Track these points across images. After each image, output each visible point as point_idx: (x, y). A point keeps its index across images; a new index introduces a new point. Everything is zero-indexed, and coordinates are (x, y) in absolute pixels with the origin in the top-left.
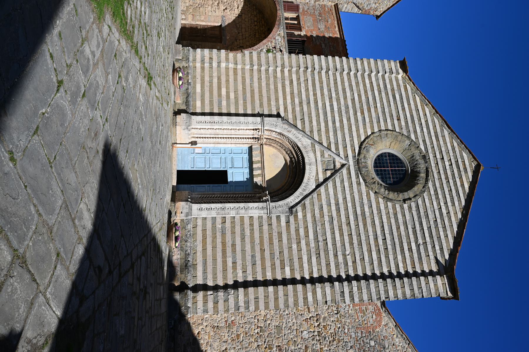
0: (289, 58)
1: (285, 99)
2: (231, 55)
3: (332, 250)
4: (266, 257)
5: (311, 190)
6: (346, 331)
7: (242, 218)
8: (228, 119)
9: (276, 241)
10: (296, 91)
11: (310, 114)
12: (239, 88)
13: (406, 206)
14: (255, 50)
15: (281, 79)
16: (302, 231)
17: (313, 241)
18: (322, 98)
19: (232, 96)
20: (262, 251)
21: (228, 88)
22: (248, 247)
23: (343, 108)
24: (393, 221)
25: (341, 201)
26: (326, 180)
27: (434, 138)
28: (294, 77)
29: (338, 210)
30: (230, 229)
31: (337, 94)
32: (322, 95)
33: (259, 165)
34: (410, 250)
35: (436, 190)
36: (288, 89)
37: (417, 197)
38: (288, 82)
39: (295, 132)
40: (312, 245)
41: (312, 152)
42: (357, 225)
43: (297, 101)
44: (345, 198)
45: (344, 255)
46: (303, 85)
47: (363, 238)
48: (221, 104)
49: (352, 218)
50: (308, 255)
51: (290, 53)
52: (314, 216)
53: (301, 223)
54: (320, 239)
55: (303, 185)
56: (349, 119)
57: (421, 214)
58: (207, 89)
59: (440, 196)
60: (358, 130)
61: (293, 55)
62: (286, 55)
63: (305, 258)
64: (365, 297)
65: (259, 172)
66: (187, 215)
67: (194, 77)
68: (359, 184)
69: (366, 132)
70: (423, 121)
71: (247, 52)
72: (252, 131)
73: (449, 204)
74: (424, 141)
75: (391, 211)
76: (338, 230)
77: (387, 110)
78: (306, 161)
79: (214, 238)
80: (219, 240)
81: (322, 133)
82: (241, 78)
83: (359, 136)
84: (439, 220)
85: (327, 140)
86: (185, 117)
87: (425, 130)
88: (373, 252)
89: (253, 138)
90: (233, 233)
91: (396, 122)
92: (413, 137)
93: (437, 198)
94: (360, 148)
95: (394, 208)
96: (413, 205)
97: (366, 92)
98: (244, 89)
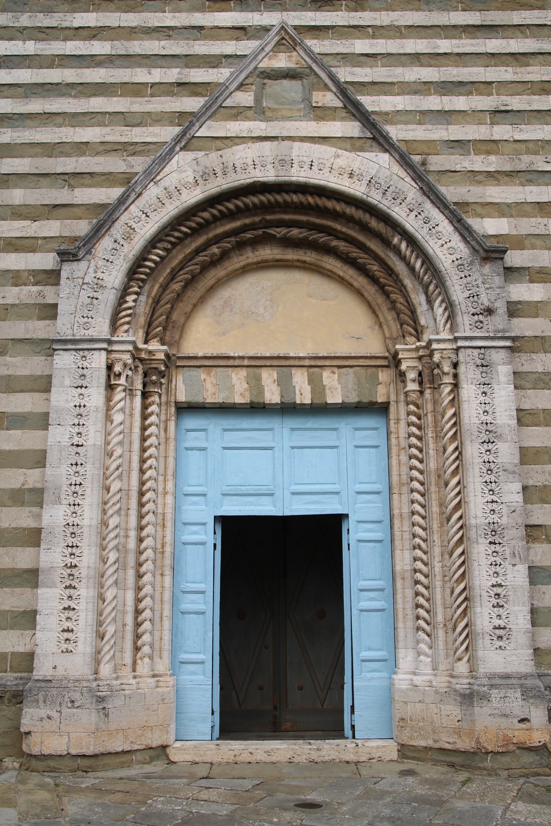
8: (58, 501)
39: (132, 207)
44: (417, 59)
49: (494, 45)
52: (494, 177)
55: (375, 198)
72: (119, 395)
76: (544, 98)
78: (269, 175)
85: (171, 94)
86: (43, 712)
89: (145, 395)
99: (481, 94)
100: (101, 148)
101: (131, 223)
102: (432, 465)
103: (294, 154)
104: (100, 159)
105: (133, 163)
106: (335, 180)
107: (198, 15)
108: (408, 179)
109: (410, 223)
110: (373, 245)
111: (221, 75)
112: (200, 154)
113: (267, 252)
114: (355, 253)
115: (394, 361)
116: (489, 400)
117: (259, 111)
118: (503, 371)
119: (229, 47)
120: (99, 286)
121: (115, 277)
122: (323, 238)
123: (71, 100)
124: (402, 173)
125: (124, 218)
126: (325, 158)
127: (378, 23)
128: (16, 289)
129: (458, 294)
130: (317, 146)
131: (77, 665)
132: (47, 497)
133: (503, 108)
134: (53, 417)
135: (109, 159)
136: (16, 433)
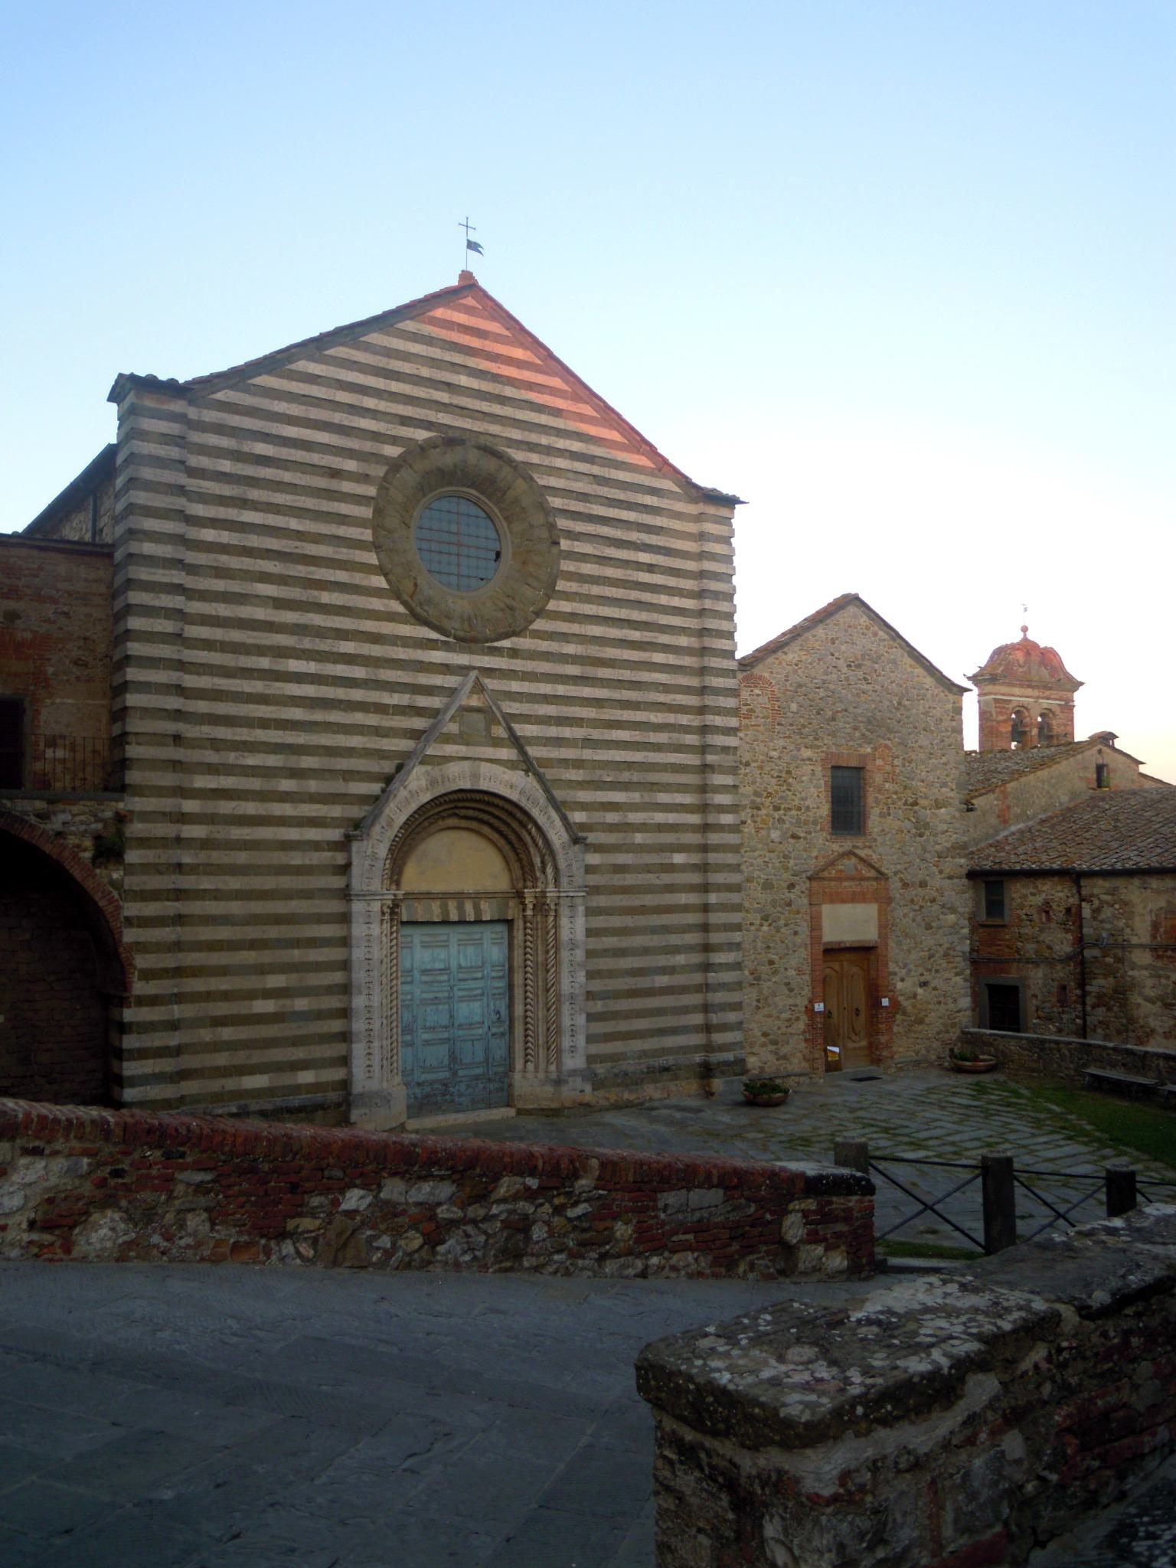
0: (140, 791)
2: (139, 987)
8: (360, 993)
10: (255, 784)
12: (251, 961)
13: (565, 544)
14: (118, 908)
16: (612, 817)
20: (643, 910)
21: (251, 995)
22: (638, 941)
23: (307, 643)
24: (596, 590)
26: (517, 742)
27: (395, 386)
28: (201, 782)
30: (607, 981)
31: (260, 650)
33: (452, 905)
34: (651, 568)
36: (251, 808)
38: (222, 803)
39: (392, 805)
40: (636, 797)
41: (444, 767)
43: (287, 785)
44: (546, 699)
46: (232, 757)
47: (626, 675)
49: (587, 692)
51: (123, 788)
53: (598, 817)
54: (625, 776)
55: (523, 803)
58: (258, 1057)
59: (544, 440)
61: (133, 777)
62: (137, 804)
63: (660, 817)
64: (731, 703)
65: (469, 907)
66: (585, 1079)
67: (219, 1097)
68: (514, 653)
69: (378, 593)
70: (342, 397)
71: (129, 935)
74: (405, 421)
75: (573, 587)
77: (310, 503)
78: (468, 786)
80: (625, 1005)
83: (391, 617)
84: (596, 470)
85: (403, 714)
86: (363, 1111)
87: (370, 403)
88: (655, 660)
92: (392, 451)
93: (549, 450)
95: (571, 576)
96: (562, 523)
98: (253, 945)
102: (540, 959)
107: (419, 651)
109: (541, 820)
110: (515, 825)
111: (435, 702)
112: (429, 768)
113: (451, 822)
114: (503, 828)
115: (520, 895)
116: (573, 927)
117: (461, 739)
118: (581, 909)
119: (438, 680)
120: (374, 857)
121: (383, 851)
122: (486, 817)
123: (342, 713)
124: (538, 787)
125: (387, 811)
126: (504, 780)
128: (317, 854)
129: (562, 864)
131: (373, 1085)
132: (354, 990)
134: (354, 942)
136: (325, 950)
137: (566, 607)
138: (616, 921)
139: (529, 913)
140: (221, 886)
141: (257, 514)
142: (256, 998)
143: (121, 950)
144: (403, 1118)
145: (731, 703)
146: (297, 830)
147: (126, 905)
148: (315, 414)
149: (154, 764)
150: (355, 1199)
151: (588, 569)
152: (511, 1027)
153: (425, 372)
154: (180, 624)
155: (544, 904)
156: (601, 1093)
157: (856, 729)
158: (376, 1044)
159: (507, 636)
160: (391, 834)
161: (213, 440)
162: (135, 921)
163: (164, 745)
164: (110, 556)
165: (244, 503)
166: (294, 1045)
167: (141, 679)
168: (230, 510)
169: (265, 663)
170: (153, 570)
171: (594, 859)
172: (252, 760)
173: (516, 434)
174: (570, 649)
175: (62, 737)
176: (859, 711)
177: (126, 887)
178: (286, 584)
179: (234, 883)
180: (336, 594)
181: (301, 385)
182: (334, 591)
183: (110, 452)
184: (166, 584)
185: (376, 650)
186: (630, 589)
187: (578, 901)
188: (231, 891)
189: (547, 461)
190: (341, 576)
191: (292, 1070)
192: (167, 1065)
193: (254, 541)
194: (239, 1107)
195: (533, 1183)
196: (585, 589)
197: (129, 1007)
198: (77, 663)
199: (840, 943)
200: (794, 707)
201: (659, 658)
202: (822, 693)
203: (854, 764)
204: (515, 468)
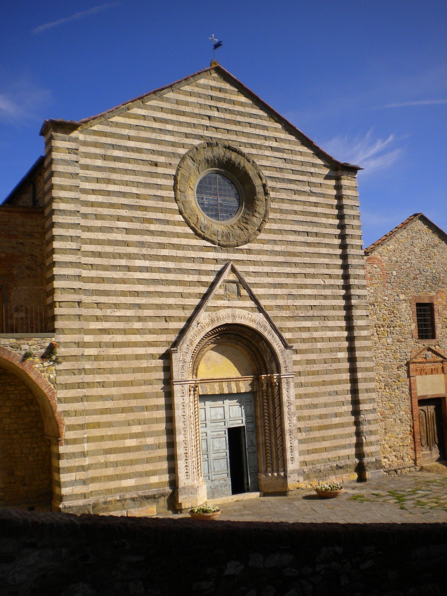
0: (63, 331)
1: (135, 344)
2: (67, 435)
3: (321, 301)
4: (330, 380)
5: (265, 319)
6: (386, 298)
7: (300, 408)
8: (180, 433)
9: (316, 367)
11: (159, 307)
13: (272, 194)
14: (54, 393)
15: (99, 349)
16: (305, 335)
17: (314, 322)
18: (130, 283)
19: (137, 429)
20: (324, 383)
21: (124, 437)
23: (144, 251)
24: (290, 217)
25: (270, 280)
26: (253, 297)
28: (94, 325)
29: (281, 286)
30: (308, 422)
31: (120, 256)
32: (124, 281)
35: (252, 146)
36: (119, 338)
37: (261, 175)
38: (105, 336)
39: (192, 333)
40: (316, 323)
42: (296, 264)
43: (137, 325)
44: (268, 274)
45: (325, 287)
46: (108, 312)
47: (307, 260)
48: (151, 445)
49: (288, 270)
50: (326, 330)
51: (54, 331)
54: (311, 313)
56: (162, 246)
57: (280, 176)
58: (129, 469)
59: (259, 142)
60: (178, 235)
61: (58, 324)
63: (329, 334)
64: (362, 272)
65: (233, 385)
67: (109, 491)
68: (249, 251)
71: (60, 408)
73: (266, 133)
74: (187, 135)
75: (278, 216)
77: (142, 179)
78: (230, 321)
79: (314, 440)
80: (317, 434)
81: (185, 291)
82: (105, 416)
85: (195, 286)
86: (184, 497)
87: (169, 127)
90: (310, 418)
91: (160, 170)
92: (182, 151)
93: (260, 147)
94: (204, 238)
95: (275, 210)
97: (112, 206)
98: (123, 410)
99: (284, 288)
100: (175, 306)
101: (192, 339)
102: (271, 412)
103: (237, 313)
104: (175, 311)
105: (186, 313)
106: (248, 322)
107: (201, 253)
108: (268, 322)
112: (210, 313)
118: (292, 384)
121: (188, 358)
123: (164, 287)
127: (256, 260)
129: (281, 361)
130: (243, 310)
133: (291, 294)
135: (178, 311)
137: (275, 226)
138: (310, 390)
139: (264, 388)
140: (106, 380)
141: (116, 186)
142: (127, 439)
143: (56, 415)
144: (206, 499)
145: (362, 272)
146: (144, 348)
147: (59, 391)
148: (144, 134)
149: (68, 317)
150: (232, 568)
151: (285, 206)
152: (258, 449)
153: (197, 111)
154: (79, 244)
155: (272, 383)
156: (306, 482)
157: (427, 283)
158: (190, 461)
159: (246, 243)
160: (192, 348)
161: (93, 150)
162: (63, 400)
163: (74, 307)
164: (43, 213)
165: (109, 181)
166: (148, 462)
167: (61, 273)
168: (102, 185)
169: (123, 262)
170: (65, 217)
171: (297, 357)
172: (119, 313)
173: (244, 140)
174: (278, 248)
175: (21, 306)
176: (428, 274)
177: (58, 382)
178: (132, 221)
179: (113, 378)
180: (157, 225)
181: (135, 120)
182: (157, 224)
183: (42, 160)
184: (72, 224)
185: (180, 253)
186: (307, 215)
187: (291, 380)
188: (110, 382)
189: (261, 152)
190: (160, 216)
191: (146, 476)
192: (81, 475)
193: (114, 200)
194: (120, 497)
195: (339, 549)
196: (284, 216)
197: (62, 445)
198: (29, 268)
199: (426, 396)
200: (394, 273)
201: (324, 250)
202: (408, 265)
203: (426, 301)
204: (244, 156)
